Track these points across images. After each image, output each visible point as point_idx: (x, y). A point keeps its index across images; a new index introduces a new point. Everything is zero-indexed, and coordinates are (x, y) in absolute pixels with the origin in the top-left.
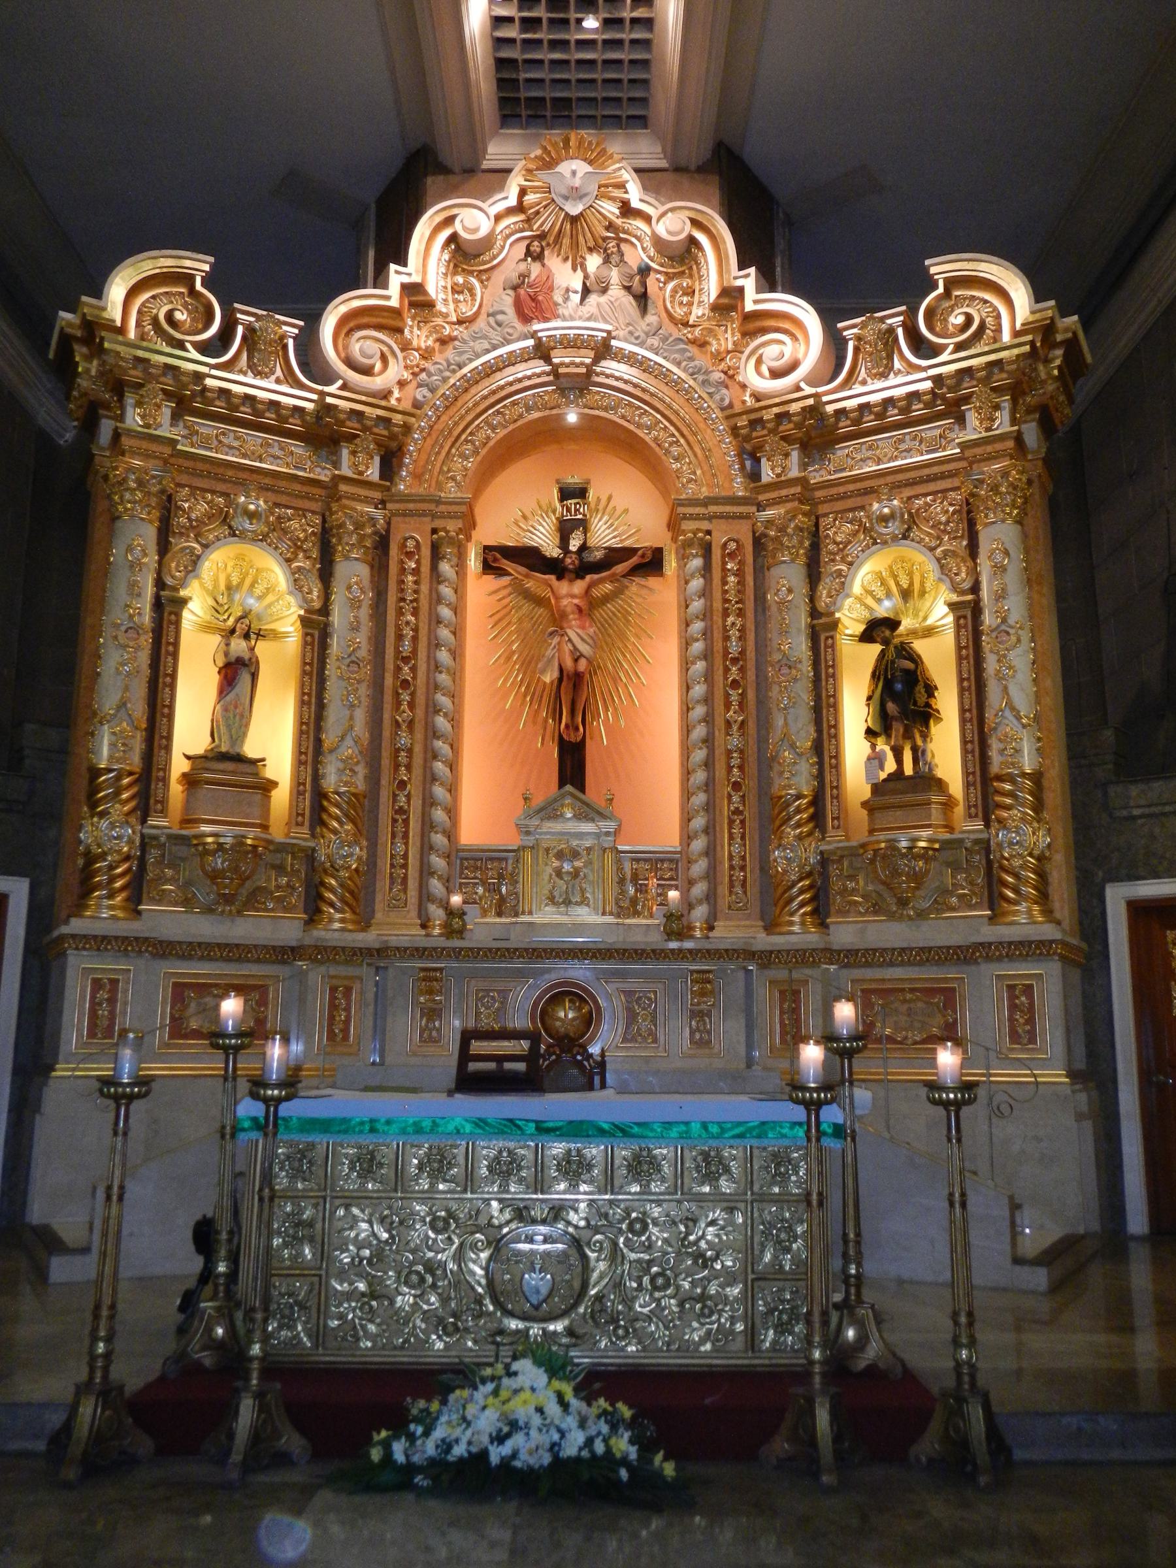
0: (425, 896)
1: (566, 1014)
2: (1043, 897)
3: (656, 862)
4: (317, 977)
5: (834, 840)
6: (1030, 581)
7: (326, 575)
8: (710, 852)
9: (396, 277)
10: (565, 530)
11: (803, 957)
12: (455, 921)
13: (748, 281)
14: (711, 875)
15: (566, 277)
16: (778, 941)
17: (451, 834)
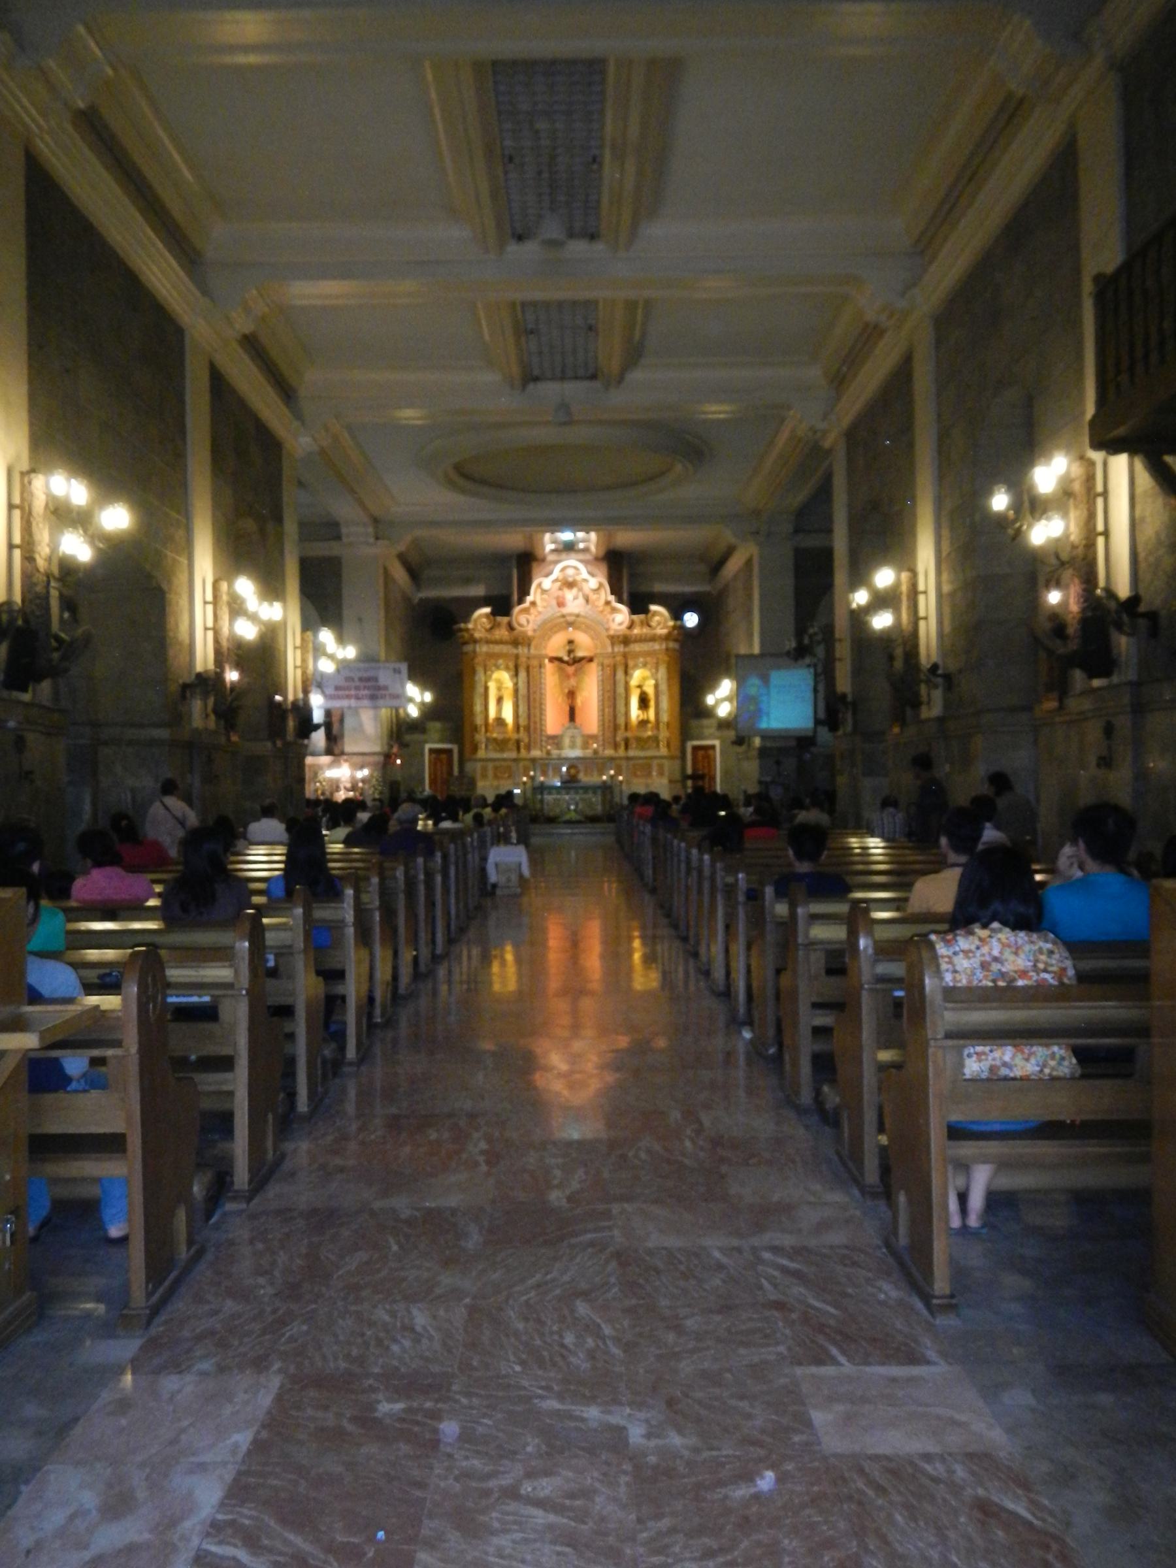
0: (541, 746)
1: (573, 771)
2: (668, 746)
3: (593, 737)
4: (521, 764)
5: (629, 734)
6: (669, 679)
7: (516, 674)
8: (603, 734)
9: (529, 599)
10: (570, 652)
11: (620, 758)
12: (548, 753)
13: (612, 598)
14: (604, 740)
15: (569, 595)
16: (617, 755)
17: (545, 731)
